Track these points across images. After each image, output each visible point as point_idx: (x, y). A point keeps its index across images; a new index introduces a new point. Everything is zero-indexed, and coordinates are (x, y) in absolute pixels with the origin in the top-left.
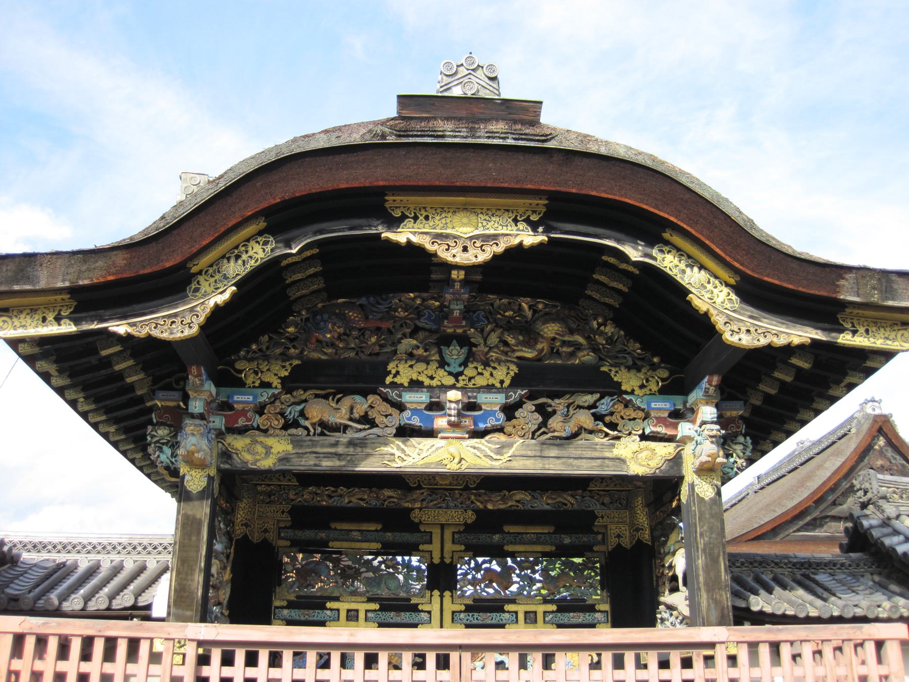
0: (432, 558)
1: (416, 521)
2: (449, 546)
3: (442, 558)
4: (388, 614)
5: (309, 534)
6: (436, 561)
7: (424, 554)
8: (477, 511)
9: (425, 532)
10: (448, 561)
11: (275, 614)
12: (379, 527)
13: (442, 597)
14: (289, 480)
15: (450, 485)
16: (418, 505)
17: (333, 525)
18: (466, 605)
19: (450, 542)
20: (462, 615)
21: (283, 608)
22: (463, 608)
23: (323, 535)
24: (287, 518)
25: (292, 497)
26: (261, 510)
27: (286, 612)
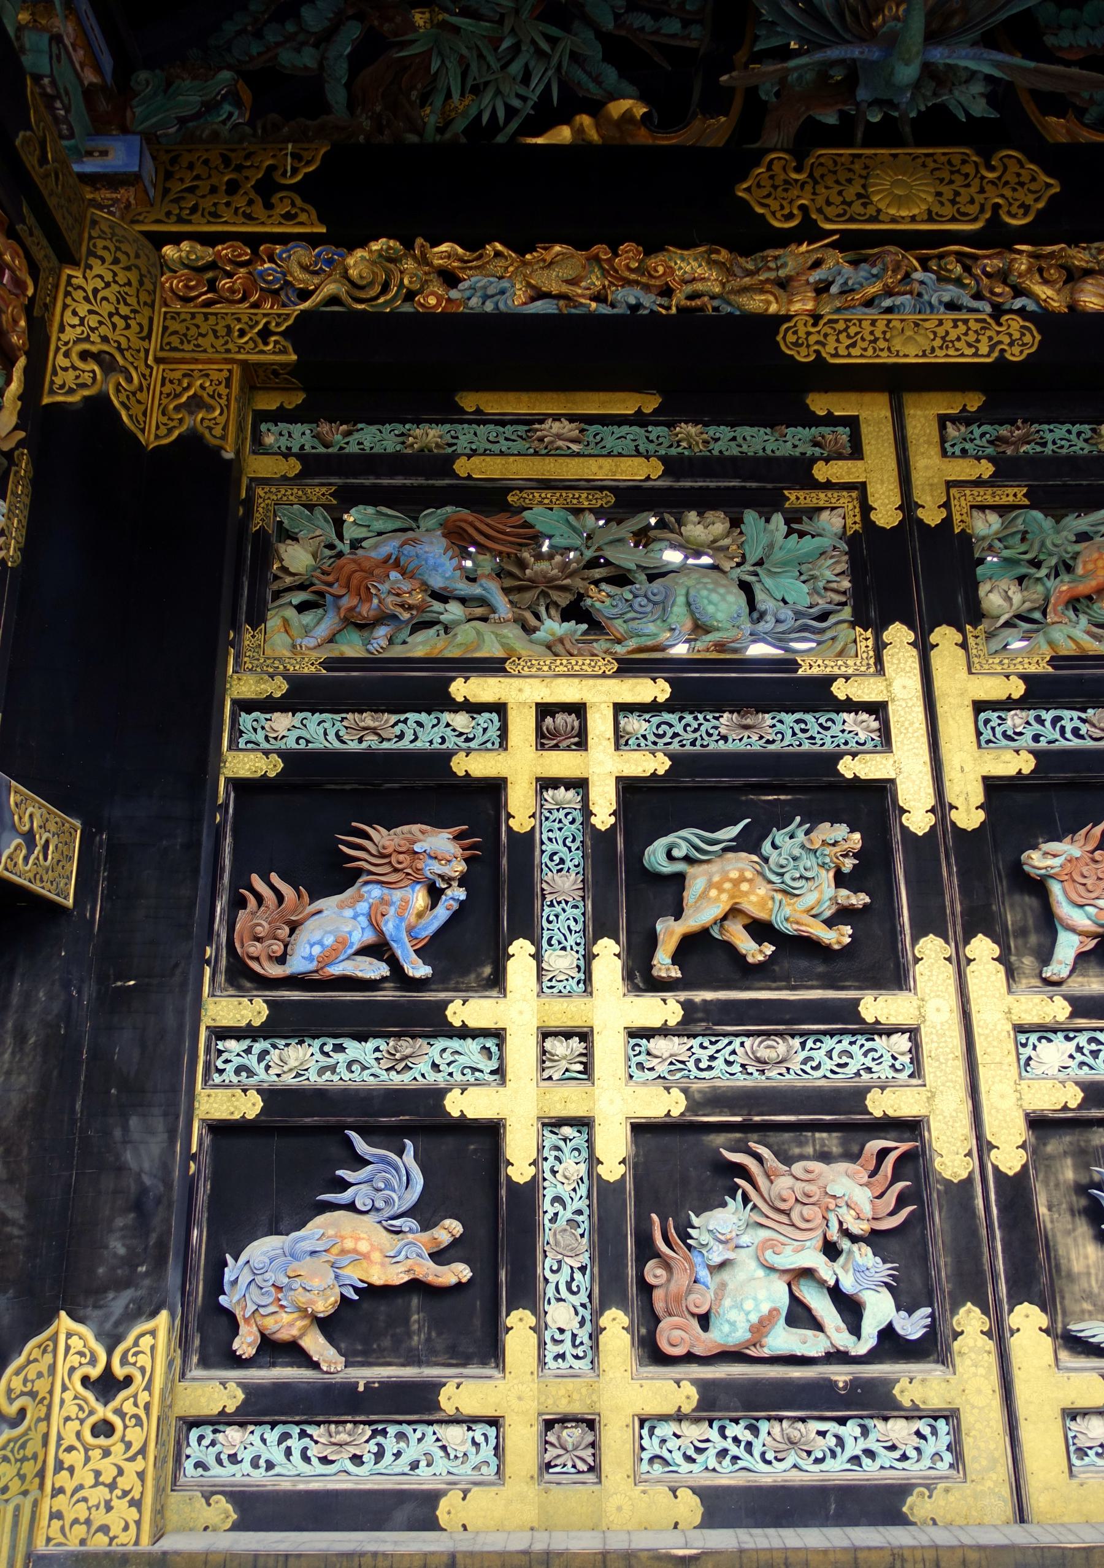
0: (866, 509)
1: (803, 356)
2: (929, 467)
3: (908, 505)
4: (707, 722)
5: (374, 438)
6: (886, 515)
7: (833, 496)
8: (1042, 319)
9: (831, 420)
10: (932, 517)
11: (237, 732)
12: (650, 403)
13: (924, 649)
14: (288, 217)
15: (930, 220)
16: (803, 304)
17: (469, 402)
18: (1025, 677)
19: (935, 451)
20: (1015, 719)
21: (268, 705)
22: (1018, 689)
23: (430, 435)
24: (279, 354)
25: (300, 278)
26: (174, 326)
27: (282, 722)
